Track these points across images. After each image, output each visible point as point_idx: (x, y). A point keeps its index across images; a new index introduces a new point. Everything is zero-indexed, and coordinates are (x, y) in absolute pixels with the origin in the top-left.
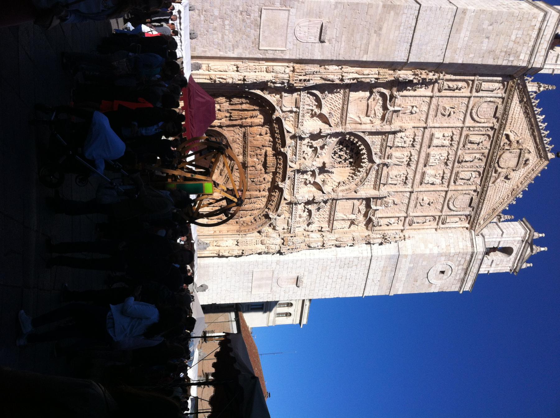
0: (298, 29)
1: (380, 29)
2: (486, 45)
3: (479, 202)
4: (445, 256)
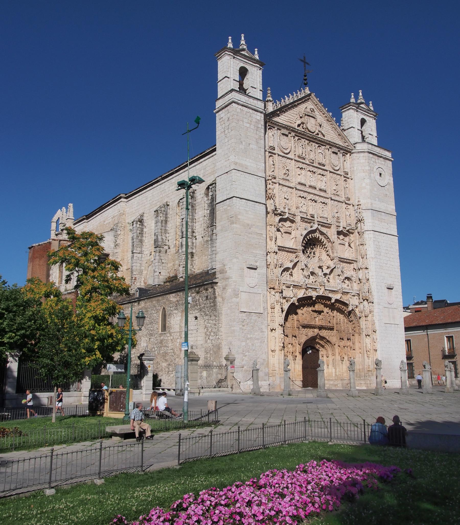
0: (251, 285)
1: (248, 225)
2: (253, 146)
3: (335, 147)
4: (370, 173)
